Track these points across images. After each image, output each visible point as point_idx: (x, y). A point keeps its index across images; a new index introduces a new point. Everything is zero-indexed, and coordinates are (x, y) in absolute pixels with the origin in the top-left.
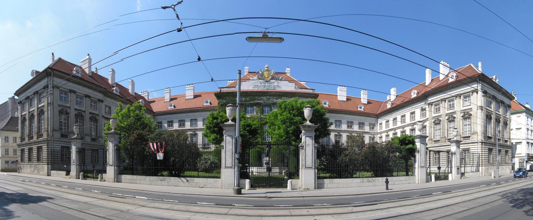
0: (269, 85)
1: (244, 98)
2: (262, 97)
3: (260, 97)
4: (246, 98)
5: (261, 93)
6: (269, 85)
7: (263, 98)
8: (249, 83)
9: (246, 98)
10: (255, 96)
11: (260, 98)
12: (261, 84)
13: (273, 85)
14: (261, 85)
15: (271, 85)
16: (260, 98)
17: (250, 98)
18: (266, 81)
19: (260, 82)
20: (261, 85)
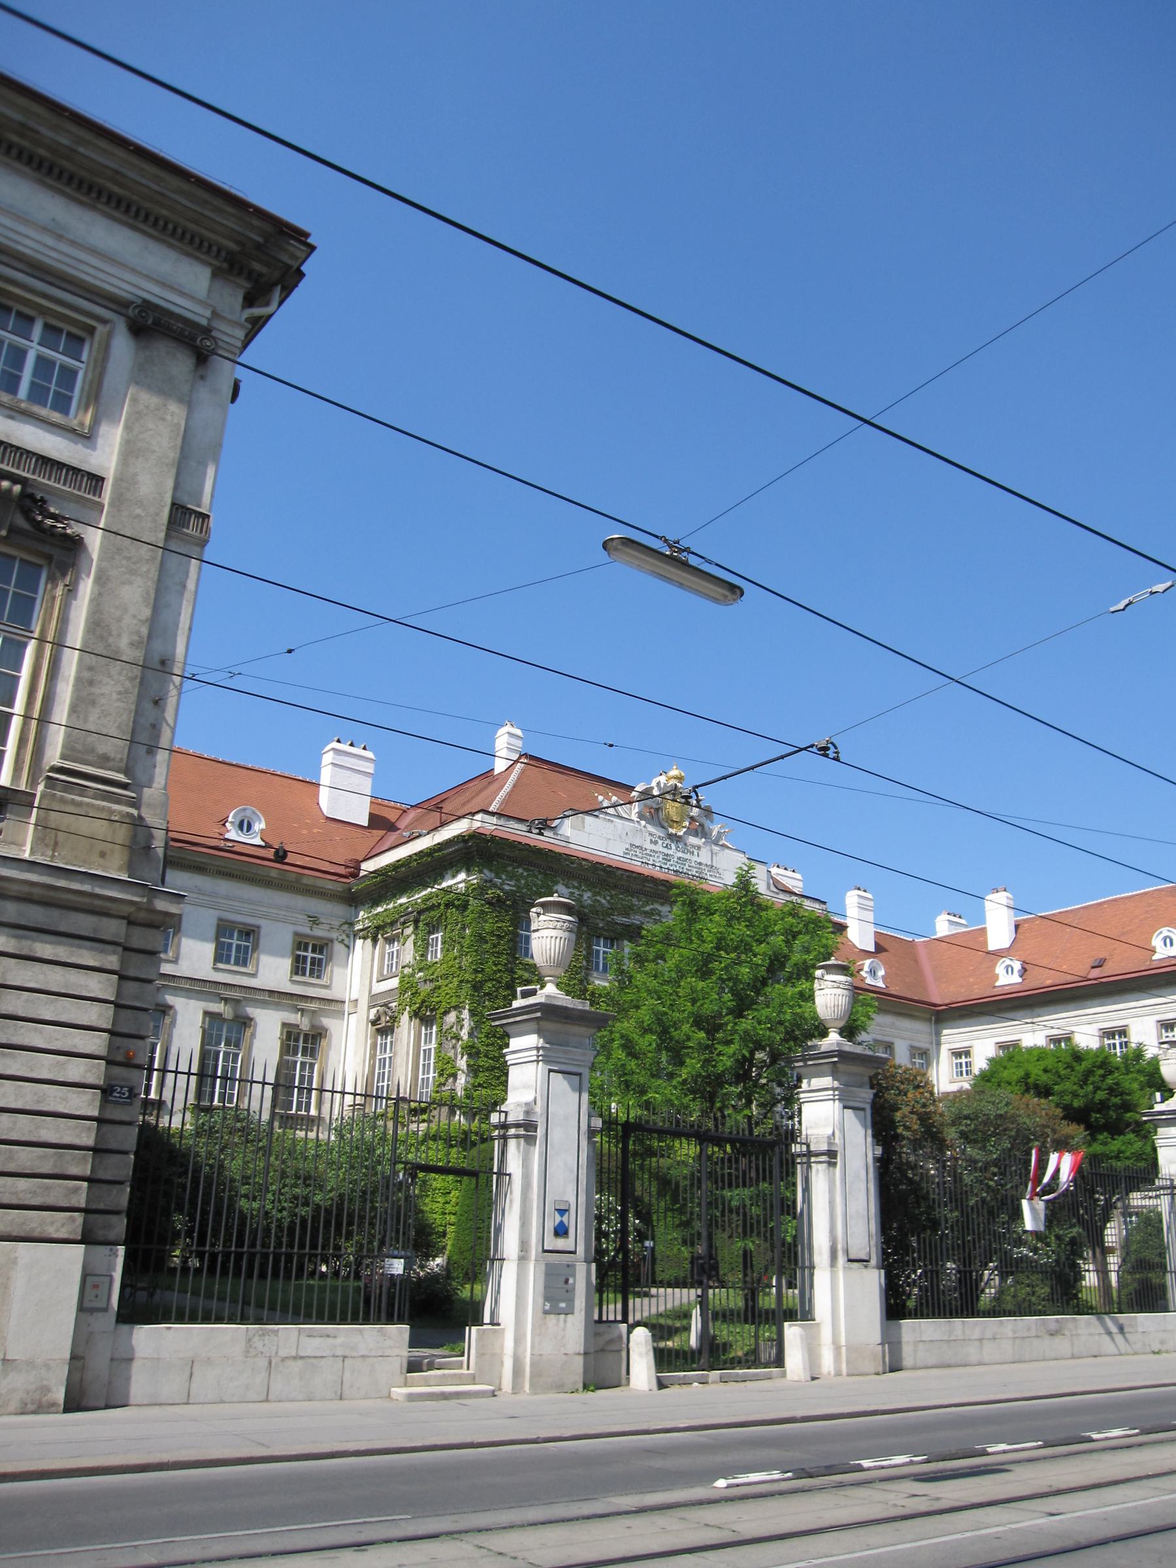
0: (680, 854)
1: (589, 894)
2: (657, 906)
3: (648, 904)
4: (595, 894)
5: (660, 888)
6: (680, 854)
7: (660, 908)
8: (612, 825)
9: (595, 894)
10: (633, 893)
11: (647, 908)
12: (656, 843)
13: (695, 858)
14: (653, 847)
15: (687, 856)
16: (647, 908)
17: (611, 896)
18: (671, 837)
19: (651, 834)
20: (653, 847)
